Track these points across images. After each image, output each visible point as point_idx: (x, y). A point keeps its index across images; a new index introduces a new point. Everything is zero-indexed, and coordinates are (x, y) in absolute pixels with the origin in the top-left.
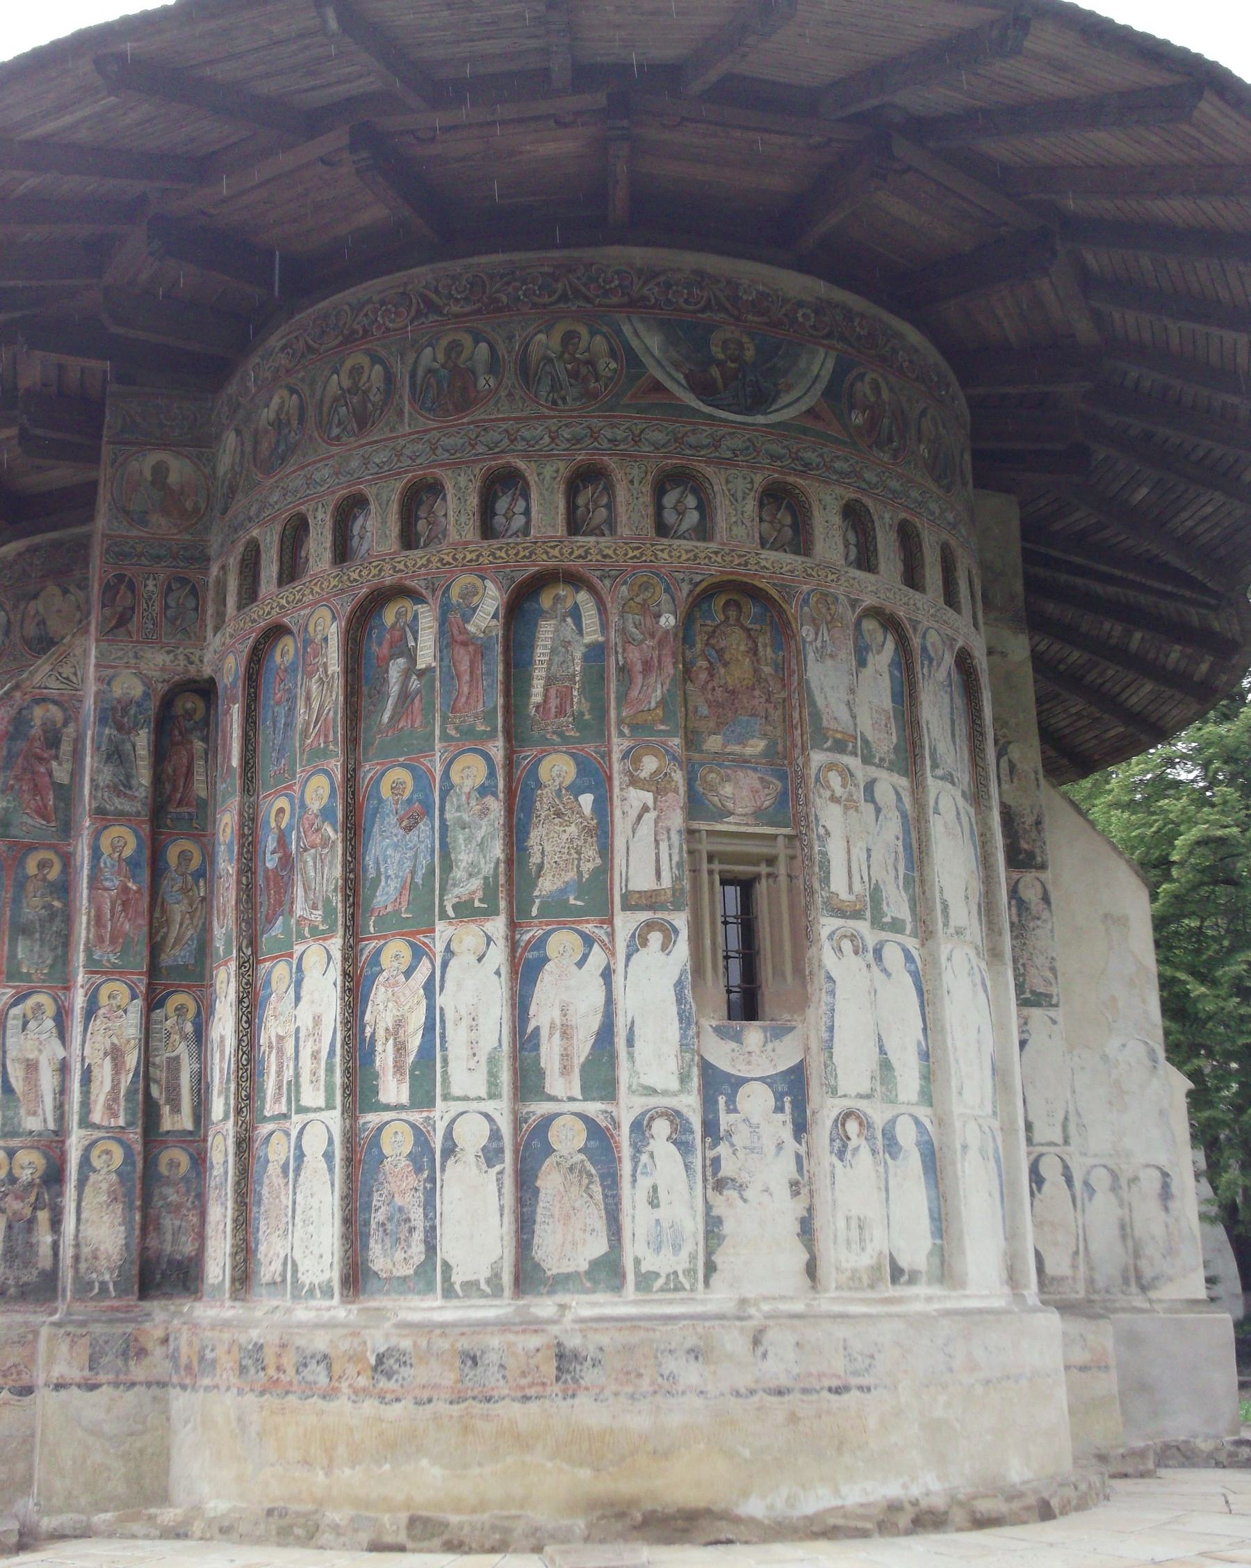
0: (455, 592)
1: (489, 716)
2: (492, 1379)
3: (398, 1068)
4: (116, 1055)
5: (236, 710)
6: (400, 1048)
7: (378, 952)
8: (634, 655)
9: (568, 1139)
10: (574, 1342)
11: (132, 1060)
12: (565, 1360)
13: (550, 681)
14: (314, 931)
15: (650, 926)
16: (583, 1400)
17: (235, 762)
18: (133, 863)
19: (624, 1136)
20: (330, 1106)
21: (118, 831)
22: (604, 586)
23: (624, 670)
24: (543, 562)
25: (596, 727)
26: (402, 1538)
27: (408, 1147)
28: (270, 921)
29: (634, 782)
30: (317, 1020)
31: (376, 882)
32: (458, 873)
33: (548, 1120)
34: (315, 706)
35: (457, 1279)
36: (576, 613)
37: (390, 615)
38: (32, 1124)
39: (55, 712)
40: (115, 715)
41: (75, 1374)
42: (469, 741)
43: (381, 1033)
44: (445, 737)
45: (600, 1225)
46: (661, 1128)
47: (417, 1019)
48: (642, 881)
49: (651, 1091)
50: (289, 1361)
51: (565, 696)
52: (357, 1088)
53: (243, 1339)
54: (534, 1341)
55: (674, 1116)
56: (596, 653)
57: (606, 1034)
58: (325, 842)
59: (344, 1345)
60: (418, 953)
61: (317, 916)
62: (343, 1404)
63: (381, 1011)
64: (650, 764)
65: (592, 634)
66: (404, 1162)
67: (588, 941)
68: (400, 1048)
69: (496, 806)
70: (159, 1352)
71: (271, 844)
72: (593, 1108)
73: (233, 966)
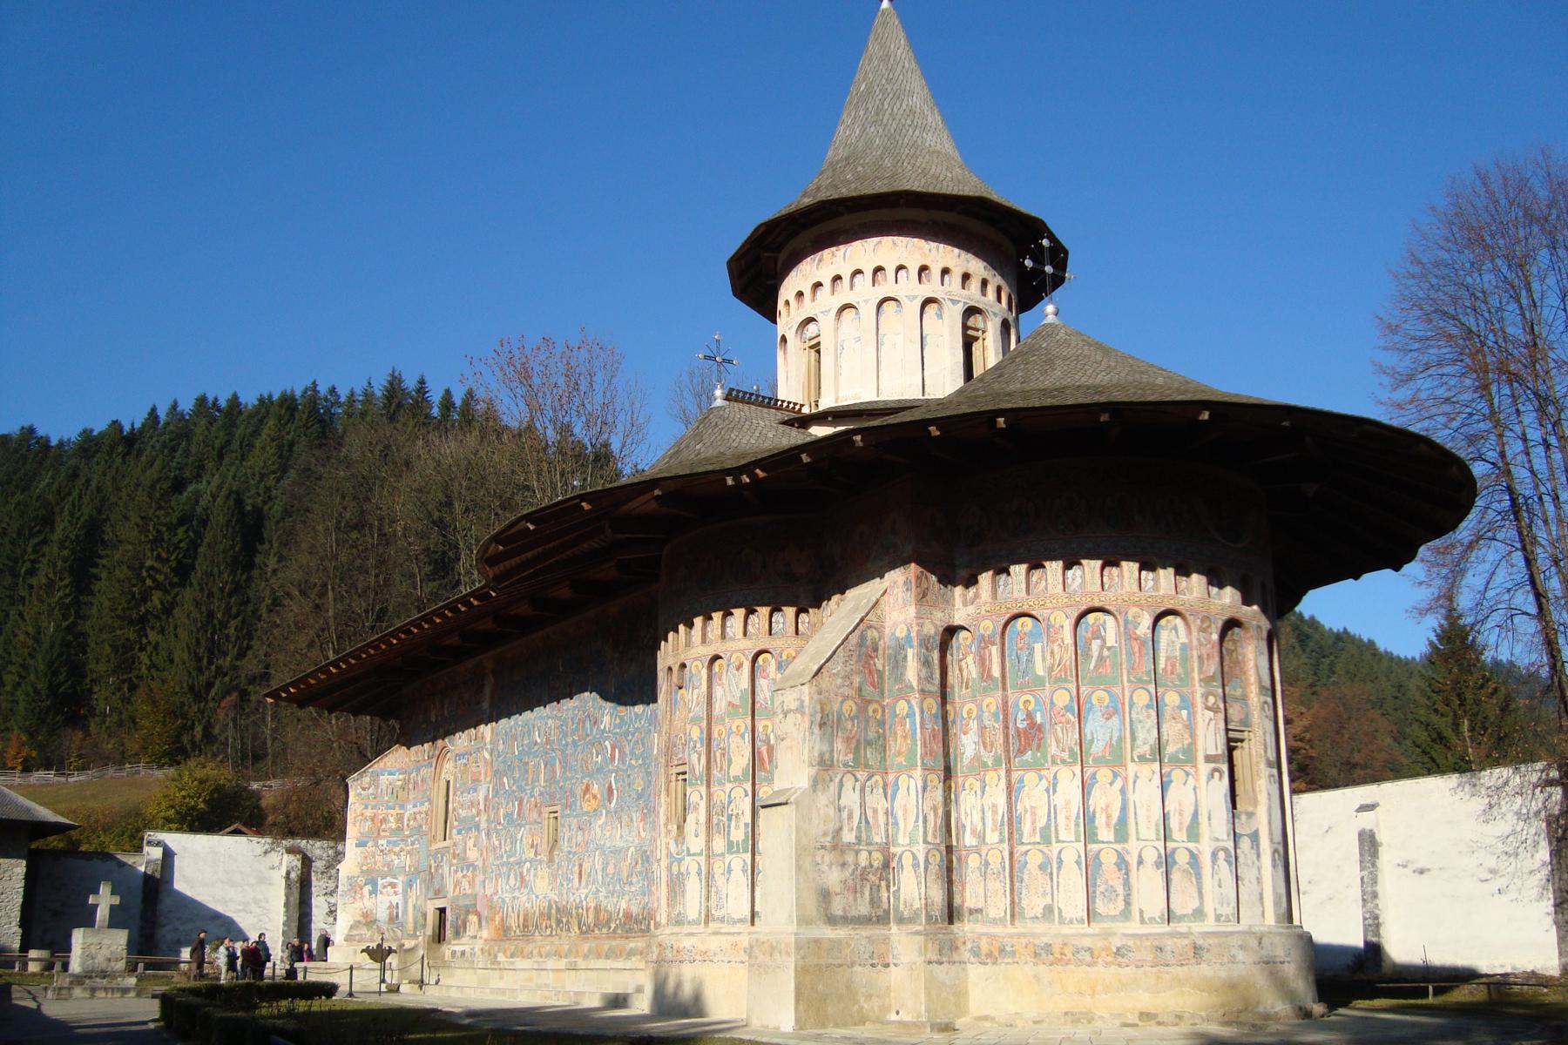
0: (1130, 615)
1: (1148, 673)
2: (1169, 956)
3: (1108, 824)
4: (935, 809)
5: (995, 650)
6: (1109, 817)
7: (1094, 774)
8: (1204, 652)
9: (1182, 858)
10: (1200, 942)
11: (940, 812)
12: (1197, 950)
13: (1168, 658)
14: (1064, 762)
15: (1216, 770)
16: (1204, 965)
17: (996, 673)
18: (935, 716)
19: (1206, 860)
20: (1078, 840)
21: (930, 701)
22: (1190, 619)
23: (1200, 657)
24: (1169, 605)
25: (1185, 680)
26: (1137, 1021)
27: (1114, 858)
28: (1021, 752)
29: (1208, 708)
30: (1068, 803)
31: (1092, 741)
32: (1139, 742)
33: (1174, 850)
34: (1057, 657)
35: (1146, 916)
36: (1175, 628)
37: (1091, 617)
38: (877, 839)
39: (875, 633)
40: (925, 642)
41: (935, 958)
42: (1138, 683)
43: (1098, 810)
44: (1129, 681)
45: (1196, 895)
46: (1221, 855)
47: (1118, 804)
48: (1212, 752)
49: (1217, 840)
50: (1068, 951)
51: (1173, 666)
52: (1089, 834)
53: (1037, 942)
54: (1186, 942)
55: (1225, 850)
56: (1184, 647)
57: (1195, 815)
58: (1068, 722)
59: (1100, 944)
60: (1115, 775)
61: (1065, 755)
62: (1100, 968)
63: (1097, 799)
64: (1211, 700)
65: (1183, 639)
66: (1113, 867)
67: (1188, 774)
68: (1109, 817)
69: (1154, 714)
70: (962, 948)
71: (1021, 716)
72: (1191, 846)
73: (1003, 773)
